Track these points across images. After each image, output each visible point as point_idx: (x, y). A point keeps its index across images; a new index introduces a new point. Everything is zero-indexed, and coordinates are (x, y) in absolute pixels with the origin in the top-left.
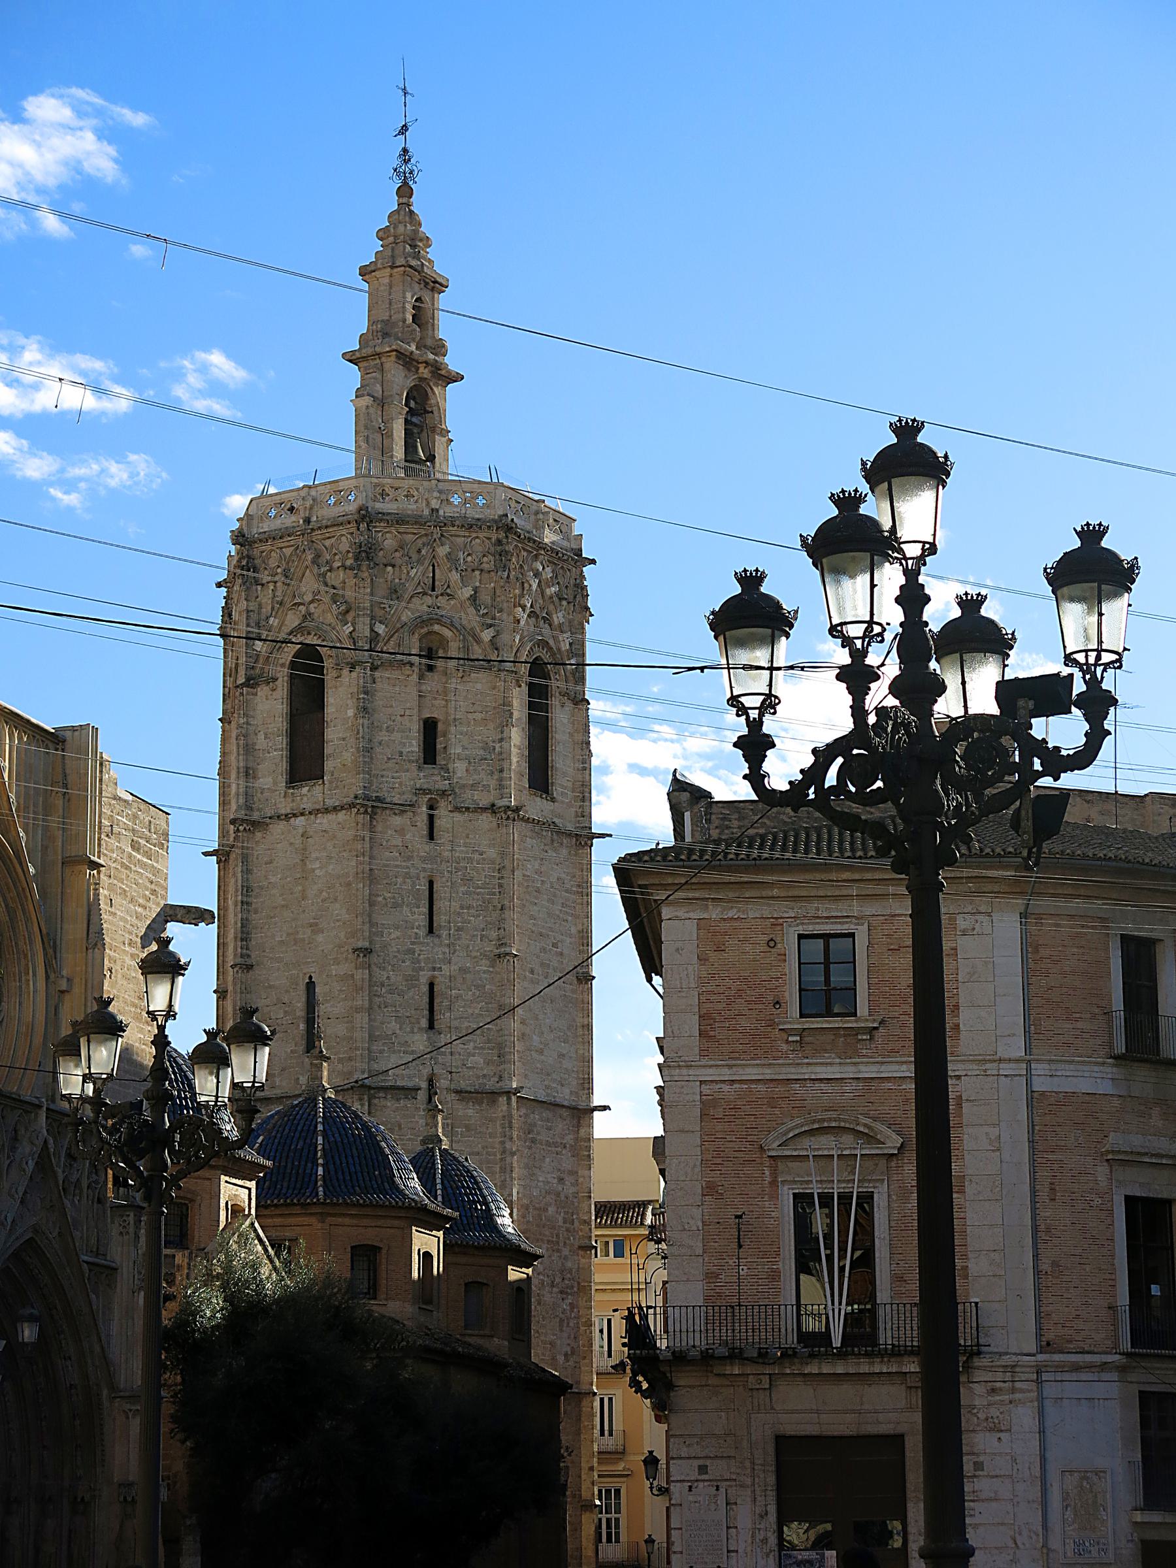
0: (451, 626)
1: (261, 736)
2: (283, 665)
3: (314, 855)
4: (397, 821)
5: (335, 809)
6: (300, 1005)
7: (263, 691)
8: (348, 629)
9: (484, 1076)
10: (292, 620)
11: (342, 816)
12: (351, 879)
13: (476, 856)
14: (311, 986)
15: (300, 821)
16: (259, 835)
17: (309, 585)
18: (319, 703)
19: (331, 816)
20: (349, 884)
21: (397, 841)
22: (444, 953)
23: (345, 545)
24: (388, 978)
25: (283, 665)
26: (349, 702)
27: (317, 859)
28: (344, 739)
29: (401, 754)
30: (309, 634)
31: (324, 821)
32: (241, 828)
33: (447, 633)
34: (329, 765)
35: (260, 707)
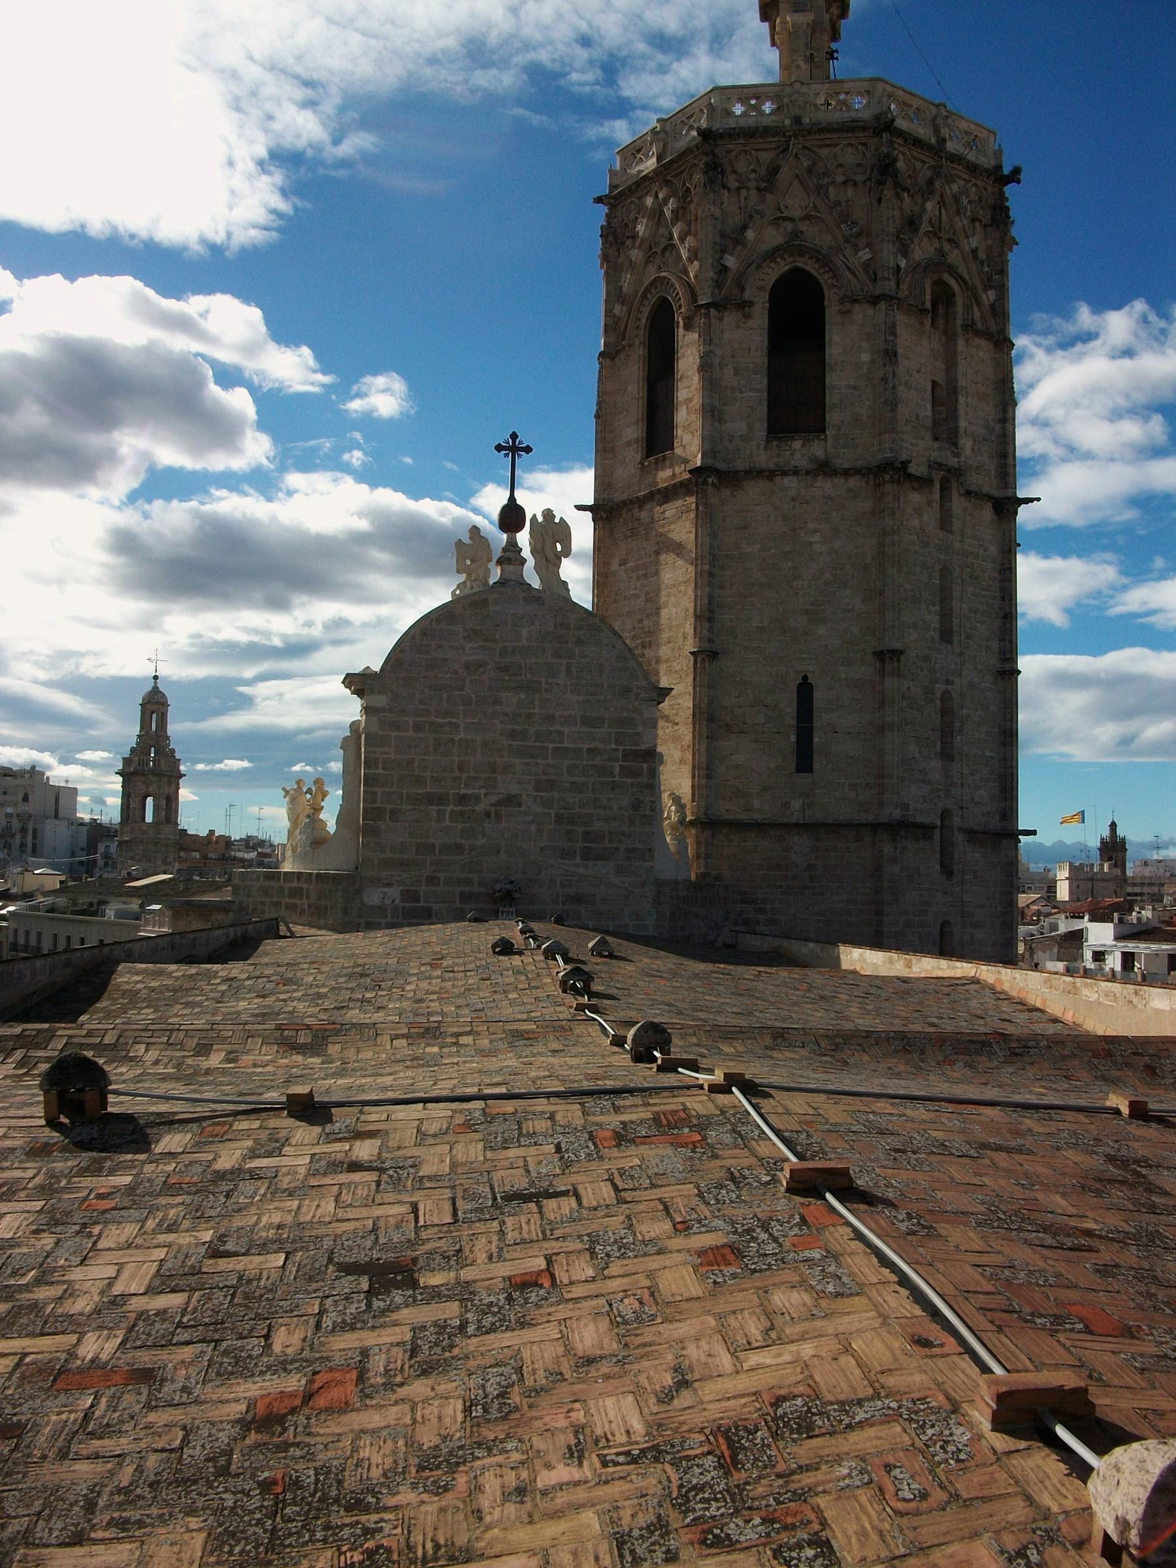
0: (959, 278)
1: (729, 371)
2: (761, 289)
3: (811, 526)
4: (916, 498)
6: (789, 708)
7: (731, 318)
8: (865, 255)
9: (989, 813)
10: (774, 237)
11: (854, 482)
13: (981, 552)
14: (805, 691)
15: (789, 482)
16: (726, 492)
18: (815, 338)
19: (839, 481)
21: (915, 522)
22: (956, 663)
23: (850, 157)
24: (908, 689)
25: (761, 289)
27: (814, 531)
28: (856, 388)
29: (918, 416)
30: (801, 255)
31: (826, 486)
32: (710, 480)
33: (953, 283)
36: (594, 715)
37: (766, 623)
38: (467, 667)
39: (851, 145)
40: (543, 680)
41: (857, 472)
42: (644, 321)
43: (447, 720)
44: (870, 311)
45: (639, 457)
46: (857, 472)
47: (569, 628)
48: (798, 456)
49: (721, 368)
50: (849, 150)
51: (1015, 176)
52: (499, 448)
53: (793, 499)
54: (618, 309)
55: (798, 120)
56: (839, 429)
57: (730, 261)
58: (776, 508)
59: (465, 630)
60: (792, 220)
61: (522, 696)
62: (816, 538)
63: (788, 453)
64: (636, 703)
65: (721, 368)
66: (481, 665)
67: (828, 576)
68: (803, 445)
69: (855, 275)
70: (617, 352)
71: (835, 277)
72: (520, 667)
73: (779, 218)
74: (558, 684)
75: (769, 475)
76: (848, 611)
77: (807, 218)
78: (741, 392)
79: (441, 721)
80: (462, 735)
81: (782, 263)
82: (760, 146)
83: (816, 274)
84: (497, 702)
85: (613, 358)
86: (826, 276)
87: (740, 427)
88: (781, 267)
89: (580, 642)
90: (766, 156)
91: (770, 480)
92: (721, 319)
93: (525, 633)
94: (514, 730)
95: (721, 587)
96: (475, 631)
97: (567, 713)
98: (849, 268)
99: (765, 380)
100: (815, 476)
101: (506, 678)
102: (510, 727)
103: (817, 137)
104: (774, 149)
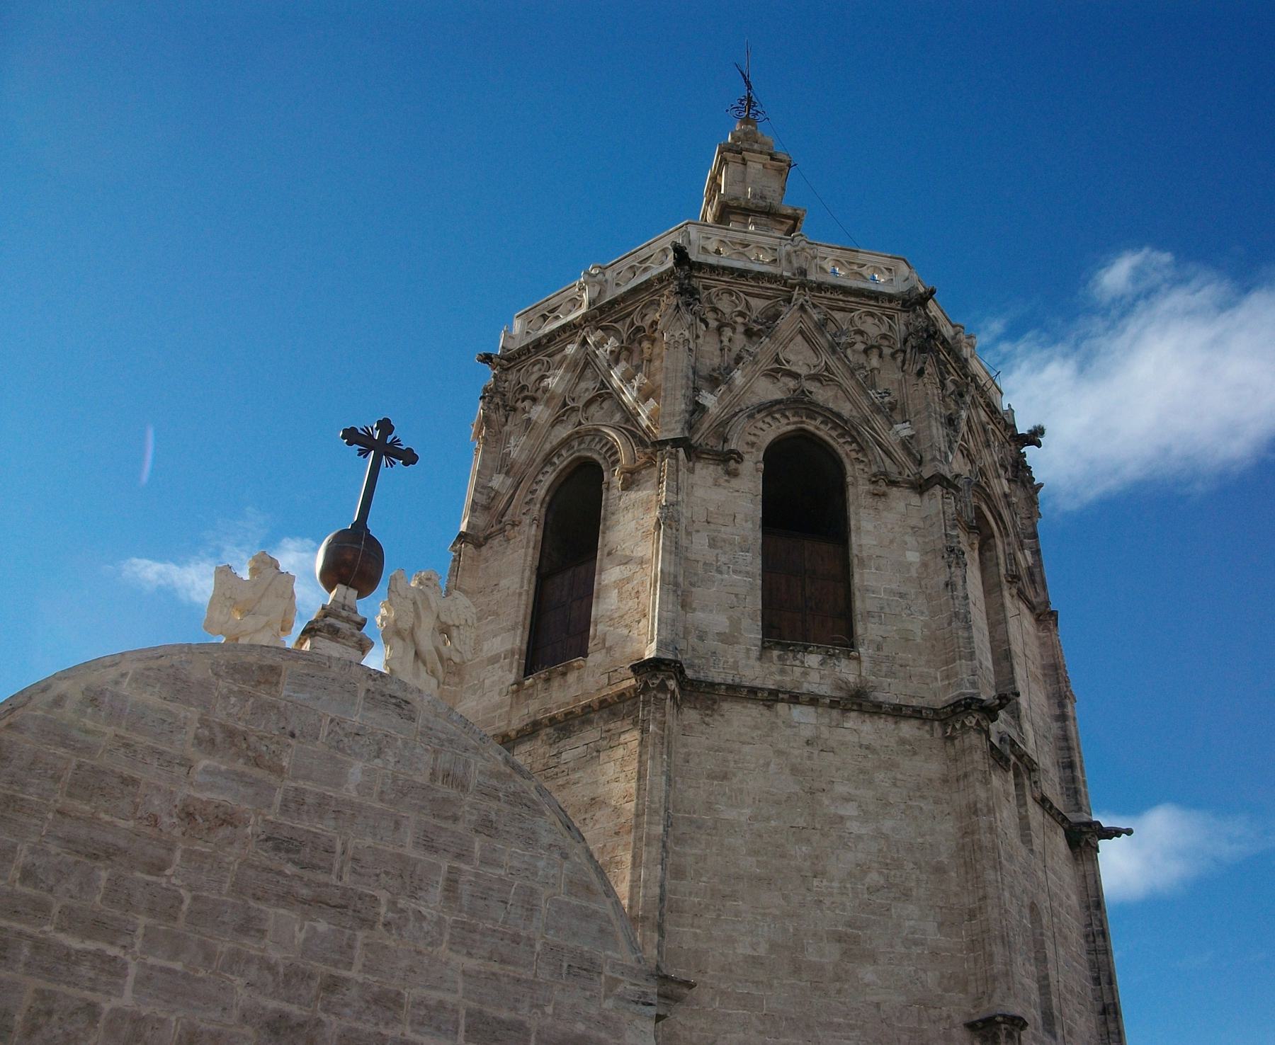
3: (841, 789)
5: (898, 712)
7: (706, 472)
8: (904, 430)
10: (769, 391)
11: (908, 729)
12: (944, 858)
15: (801, 714)
16: (691, 715)
17: (800, 358)
19: (885, 725)
20: (939, 870)
26: (908, 538)
28: (902, 595)
31: (862, 729)
34: (867, 630)
35: (699, 492)
36: (505, 1015)
37: (762, 950)
38: (188, 815)
39: (872, 315)
40: (384, 896)
41: (917, 714)
42: (541, 492)
43: (90, 945)
44: (915, 499)
45: (512, 677)
46: (917, 714)
47: (463, 787)
48: (814, 677)
49: (689, 534)
50: (869, 320)
51: (1034, 437)
52: (351, 436)
53: (808, 743)
54: (498, 481)
55: (803, 272)
56: (879, 648)
57: (709, 400)
58: (780, 753)
59: (204, 722)
60: (795, 376)
61: (322, 926)
62: (850, 810)
63: (798, 670)
64: (609, 1004)
65: (689, 534)
66: (228, 819)
67: (874, 878)
68: (823, 663)
69: (888, 454)
70: (487, 538)
71: (861, 449)
72: (329, 850)
73: (776, 371)
74: (420, 916)
75: (772, 698)
76: (916, 943)
77: (814, 378)
78: (721, 572)
79: (75, 943)
80: (127, 999)
81: (784, 421)
82: (750, 290)
83: (831, 441)
84: (249, 926)
85: (478, 546)
86: (848, 448)
87: (718, 621)
88: (782, 426)
89: (486, 826)
90: (758, 304)
91: (769, 707)
92: (691, 471)
93: (356, 771)
94: (283, 1016)
95: (679, 873)
96: (231, 734)
97: (435, 996)
98: (880, 445)
99: (759, 561)
100: (846, 710)
101: (289, 869)
102: (272, 1004)
103: (828, 295)
104: (768, 298)
